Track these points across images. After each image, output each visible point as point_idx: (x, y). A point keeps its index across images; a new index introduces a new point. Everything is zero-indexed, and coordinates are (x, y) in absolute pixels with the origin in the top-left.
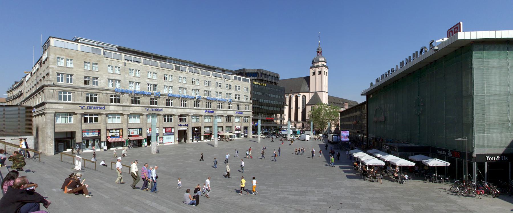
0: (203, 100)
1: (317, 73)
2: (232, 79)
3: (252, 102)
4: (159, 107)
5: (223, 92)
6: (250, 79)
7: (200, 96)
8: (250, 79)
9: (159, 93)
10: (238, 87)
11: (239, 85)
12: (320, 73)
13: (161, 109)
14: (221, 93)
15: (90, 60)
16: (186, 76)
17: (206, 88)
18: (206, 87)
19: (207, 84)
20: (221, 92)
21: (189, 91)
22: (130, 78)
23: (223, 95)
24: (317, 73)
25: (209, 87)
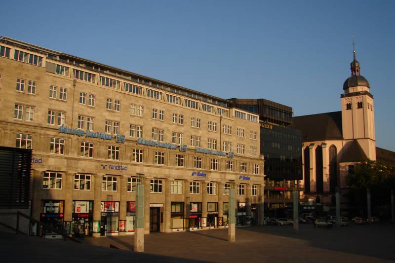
1: (355, 106)
2: (231, 116)
3: (263, 158)
4: (122, 164)
5: (219, 140)
6: (258, 116)
7: (186, 146)
8: (258, 116)
9: (124, 136)
11: (243, 126)
12: (360, 105)
13: (125, 166)
15: (26, 75)
16: (164, 107)
21: (167, 135)
22: (82, 109)
23: (218, 145)
24: (355, 106)
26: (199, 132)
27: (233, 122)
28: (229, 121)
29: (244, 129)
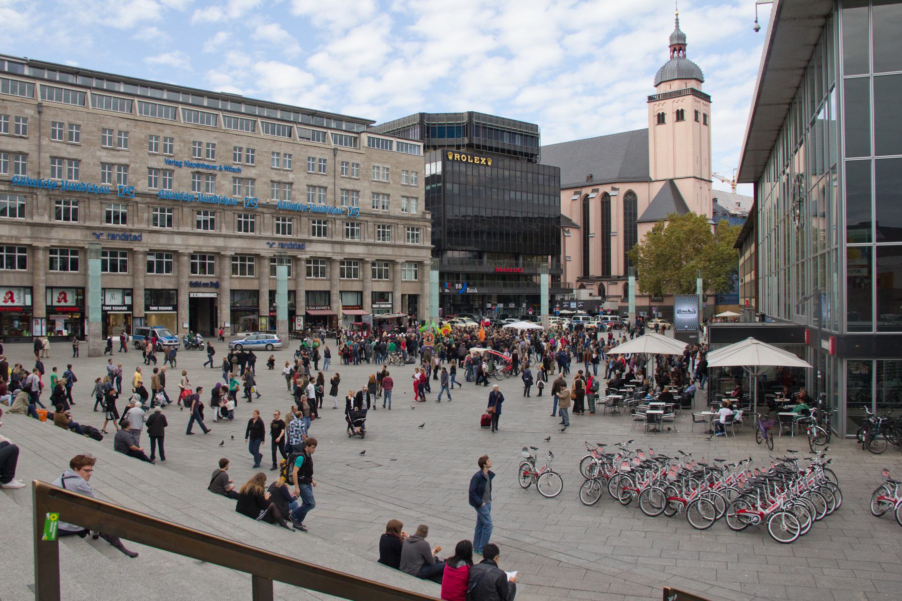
0: (265, 210)
5: (330, 187)
10: (381, 172)
11: (385, 163)
14: (325, 188)
17: (276, 174)
18: (276, 171)
19: (281, 162)
20: (325, 185)
25: (286, 172)
26: (287, 176)
27: (363, 157)
28: (355, 155)
29: (388, 166)
